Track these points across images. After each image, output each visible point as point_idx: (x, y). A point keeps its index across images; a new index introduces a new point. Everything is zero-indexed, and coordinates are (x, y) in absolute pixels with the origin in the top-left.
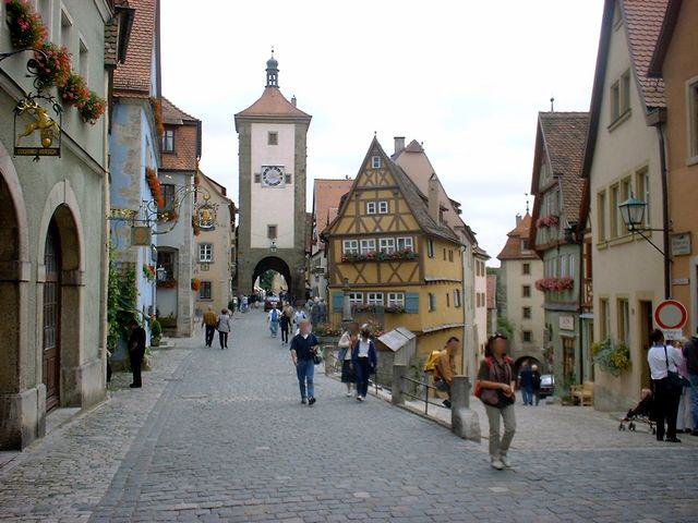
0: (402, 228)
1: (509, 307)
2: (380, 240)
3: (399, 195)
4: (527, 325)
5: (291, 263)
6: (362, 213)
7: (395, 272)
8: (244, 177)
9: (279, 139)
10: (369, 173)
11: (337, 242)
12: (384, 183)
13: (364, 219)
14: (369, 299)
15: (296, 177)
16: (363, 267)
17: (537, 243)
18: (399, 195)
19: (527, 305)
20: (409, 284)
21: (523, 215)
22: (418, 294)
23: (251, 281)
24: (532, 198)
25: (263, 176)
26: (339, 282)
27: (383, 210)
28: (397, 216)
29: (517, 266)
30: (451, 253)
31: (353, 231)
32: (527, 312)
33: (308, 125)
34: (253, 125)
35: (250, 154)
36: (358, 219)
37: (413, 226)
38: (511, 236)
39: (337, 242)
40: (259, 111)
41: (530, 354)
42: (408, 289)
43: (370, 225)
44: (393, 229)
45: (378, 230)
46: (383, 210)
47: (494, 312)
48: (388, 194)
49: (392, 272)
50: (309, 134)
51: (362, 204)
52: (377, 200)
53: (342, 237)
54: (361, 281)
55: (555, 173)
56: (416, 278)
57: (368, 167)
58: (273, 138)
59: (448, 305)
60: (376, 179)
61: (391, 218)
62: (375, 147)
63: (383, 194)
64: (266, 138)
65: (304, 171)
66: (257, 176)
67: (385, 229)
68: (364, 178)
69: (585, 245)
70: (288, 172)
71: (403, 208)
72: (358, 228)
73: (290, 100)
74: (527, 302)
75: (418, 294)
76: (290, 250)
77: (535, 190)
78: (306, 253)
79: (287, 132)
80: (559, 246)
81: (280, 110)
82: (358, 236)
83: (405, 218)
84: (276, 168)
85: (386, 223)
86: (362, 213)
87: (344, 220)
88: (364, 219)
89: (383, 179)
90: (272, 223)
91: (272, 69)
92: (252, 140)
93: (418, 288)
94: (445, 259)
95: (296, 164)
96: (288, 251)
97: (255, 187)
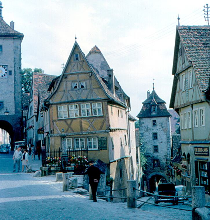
16: (71, 123)
17: (175, 105)
19: (156, 144)
29: (148, 122)
30: (121, 112)
32: (156, 149)
33: (21, 40)
38: (144, 104)
47: (139, 148)
50: (22, 44)
62: (76, 47)
68: (70, 67)
70: (10, 69)
73: (9, 25)
77: (174, 72)
80: (192, 105)
94: (119, 117)
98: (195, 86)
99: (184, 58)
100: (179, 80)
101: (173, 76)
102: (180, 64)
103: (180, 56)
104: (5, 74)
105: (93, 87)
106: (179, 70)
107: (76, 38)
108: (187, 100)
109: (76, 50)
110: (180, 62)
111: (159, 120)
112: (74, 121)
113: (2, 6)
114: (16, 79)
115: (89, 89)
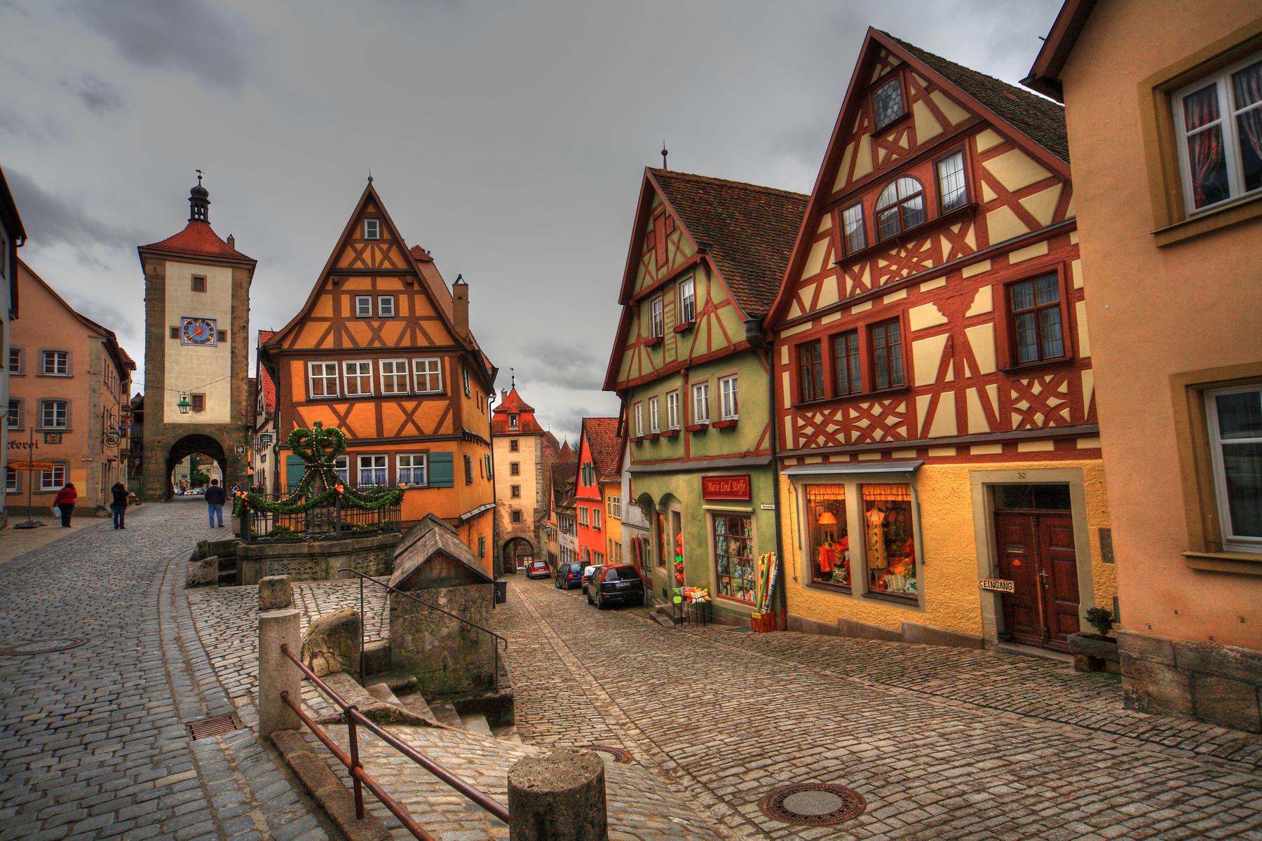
0: (421, 342)
4: (516, 503)
5: (227, 442)
6: (343, 316)
7: (410, 417)
8: (154, 330)
9: (209, 285)
10: (359, 246)
11: (297, 366)
12: (387, 265)
13: (349, 325)
15: (233, 334)
16: (348, 412)
17: (623, 377)
18: (416, 287)
19: (516, 483)
20: (436, 438)
23: (163, 466)
24: (620, 309)
25: (183, 331)
27: (387, 310)
28: (413, 322)
31: (329, 344)
32: (515, 491)
35: (163, 301)
36: (337, 324)
37: (441, 339)
39: (297, 366)
40: (178, 244)
41: (520, 535)
42: (435, 448)
43: (362, 334)
44: (406, 342)
45: (377, 344)
46: (387, 310)
48: (395, 284)
49: (403, 418)
51: (345, 300)
52: (375, 293)
53: (306, 355)
55: (700, 244)
56: (447, 428)
57: (357, 235)
58: (199, 284)
59: (482, 478)
60: (371, 257)
61: (402, 325)
62: (370, 199)
63: (384, 284)
64: (188, 283)
65: (245, 328)
67: (391, 343)
68: (349, 255)
69: (785, 350)
71: (422, 308)
72: (338, 339)
73: (225, 241)
74: (516, 480)
78: (248, 428)
79: (219, 279)
81: (215, 249)
82: (338, 353)
83: (424, 323)
84: (203, 320)
85: (391, 333)
86: (346, 312)
87: (309, 323)
88: (349, 325)
89: (386, 256)
91: (199, 199)
92: (167, 281)
93: (452, 447)
95: (233, 318)
96: (221, 428)
97: (171, 346)
98: (705, 317)
99: (667, 250)
100: (639, 318)
102: (648, 271)
103: (649, 251)
105: (418, 314)
106: (644, 287)
107: (370, 179)
108: (668, 360)
109: (371, 209)
110: (647, 267)
112: (359, 407)
113: (208, 199)
114: (236, 351)
115: (403, 319)
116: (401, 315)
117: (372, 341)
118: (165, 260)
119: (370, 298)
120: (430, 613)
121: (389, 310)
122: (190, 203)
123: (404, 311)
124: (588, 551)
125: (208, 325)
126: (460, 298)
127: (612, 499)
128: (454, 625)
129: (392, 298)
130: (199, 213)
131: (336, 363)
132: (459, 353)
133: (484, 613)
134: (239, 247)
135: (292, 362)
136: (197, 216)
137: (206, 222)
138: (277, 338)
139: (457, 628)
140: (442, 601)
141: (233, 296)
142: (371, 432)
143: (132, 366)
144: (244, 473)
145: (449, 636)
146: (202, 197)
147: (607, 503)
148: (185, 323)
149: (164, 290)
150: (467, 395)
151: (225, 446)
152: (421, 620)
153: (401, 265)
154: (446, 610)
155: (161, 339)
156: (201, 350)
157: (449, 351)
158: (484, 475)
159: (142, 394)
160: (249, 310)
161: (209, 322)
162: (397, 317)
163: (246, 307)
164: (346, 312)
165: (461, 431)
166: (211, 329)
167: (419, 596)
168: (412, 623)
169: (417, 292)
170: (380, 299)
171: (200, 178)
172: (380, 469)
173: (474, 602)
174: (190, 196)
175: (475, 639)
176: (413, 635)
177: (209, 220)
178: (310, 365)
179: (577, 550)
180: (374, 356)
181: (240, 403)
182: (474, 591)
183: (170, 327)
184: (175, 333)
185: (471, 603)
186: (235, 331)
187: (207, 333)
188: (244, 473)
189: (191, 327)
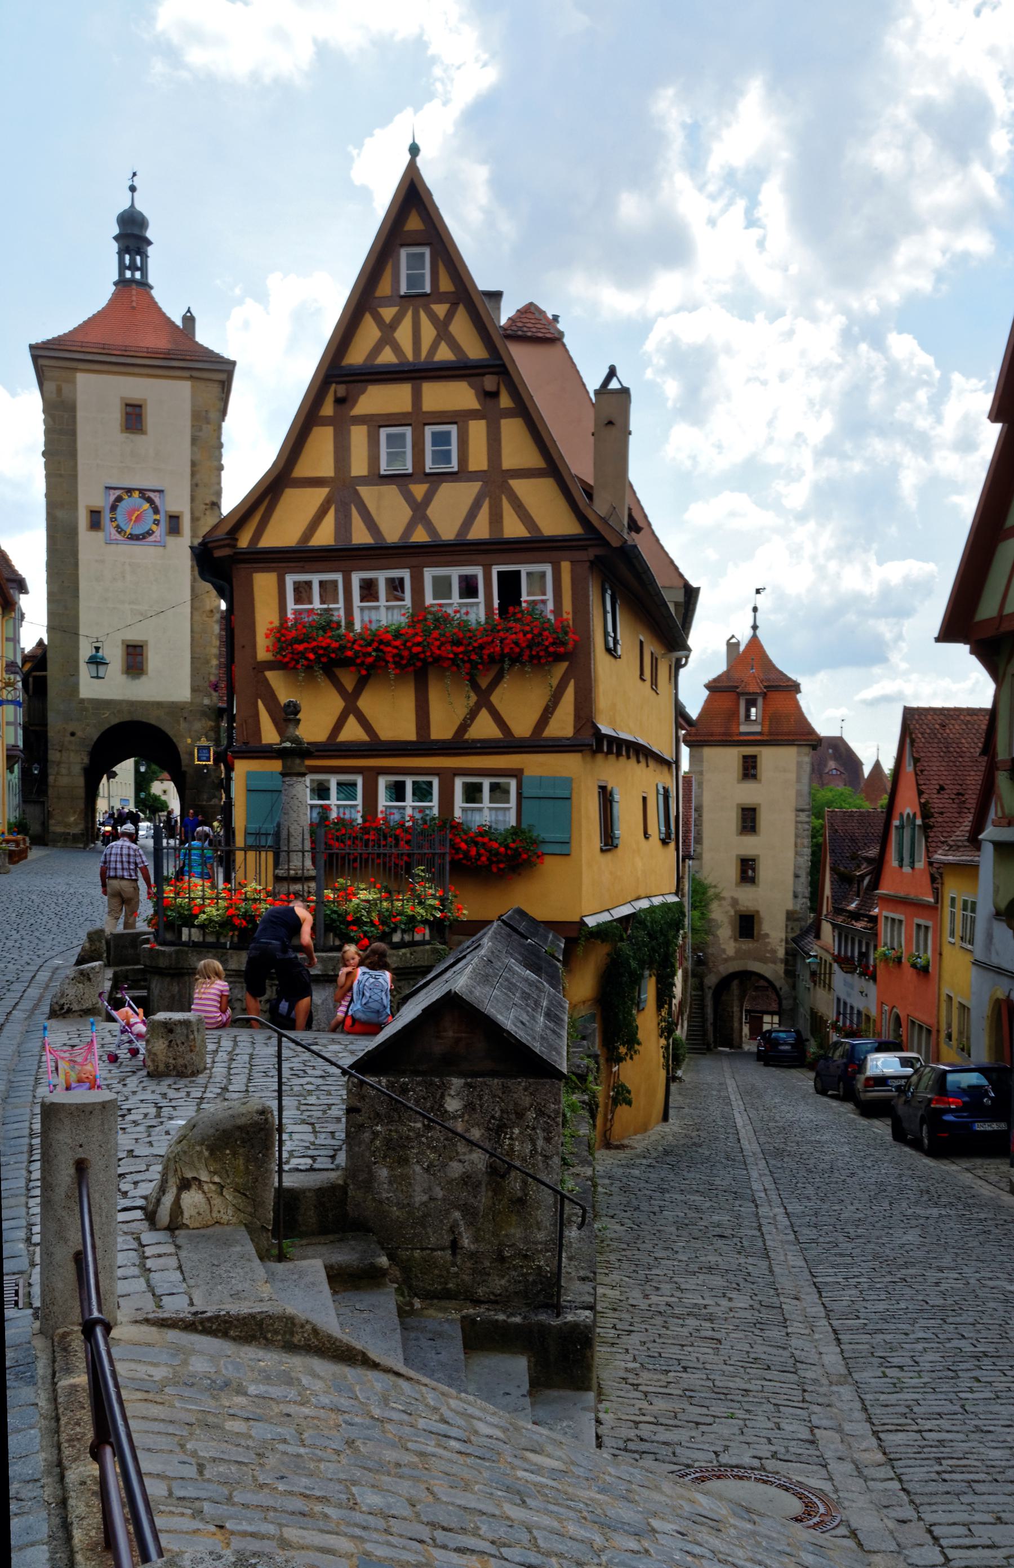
0: (513, 528)
1: (707, 856)
2: (429, 574)
3: (505, 401)
9: (151, 418)
11: (264, 583)
14: (383, 801)
15: (194, 519)
18: (505, 401)
21: (744, 636)
22: (568, 782)
26: (270, 735)
31: (325, 536)
33: (225, 387)
34: (81, 378)
39: (264, 583)
40: (94, 337)
44: (480, 531)
45: (420, 536)
54: (352, 732)
61: (475, 487)
64: (116, 416)
66: (95, 521)
67: (448, 532)
72: (343, 526)
73: (179, 322)
75: (568, 782)
76: (186, 703)
81: (160, 342)
83: (517, 485)
84: (142, 492)
86: (359, 467)
90: (133, 636)
92: (80, 414)
95: (195, 486)
96: (174, 709)
101: (998, 426)
104: (154, 527)
111: (769, 757)
113: (149, 234)
116: (473, 466)
117: (410, 528)
118: (76, 370)
119: (408, 431)
120: (428, 1128)
121: (446, 457)
122: (115, 247)
123: (478, 461)
124: (898, 1018)
125: (150, 501)
126: (610, 423)
127: (959, 904)
128: (478, 1159)
129: (453, 429)
130: (133, 267)
131: (338, 577)
132: (591, 553)
133: (540, 1143)
134: (205, 337)
135: (255, 575)
136: (128, 274)
137: (144, 285)
138: (227, 527)
139: (481, 1166)
140: (453, 1105)
141: (194, 441)
142: (407, 732)
143: (21, 586)
144: (214, 801)
145: (466, 1180)
146: (136, 232)
147: (947, 910)
148: (112, 498)
149: (73, 433)
150: (608, 650)
151: (182, 748)
152: (408, 1138)
153: (475, 351)
154: (459, 1126)
155: (72, 533)
156: (137, 549)
157: (570, 548)
158: (653, 829)
159: (46, 642)
160: (221, 468)
161: (152, 495)
162: (461, 475)
163: (216, 463)
164: (359, 467)
165: (591, 731)
166: (156, 511)
167: (404, 1090)
168: (388, 1142)
169: (508, 413)
170: (429, 430)
171: (133, 189)
172: (345, 806)
173: (520, 1115)
174: (116, 231)
175: (519, 1194)
176: (391, 1168)
177: (151, 280)
178: (290, 580)
179: (874, 1013)
180: (414, 561)
181: (208, 662)
182: (521, 1090)
183: (87, 507)
184: (95, 521)
185: (513, 1117)
186: (197, 514)
187: (151, 516)
188: (214, 801)
189: (122, 506)
